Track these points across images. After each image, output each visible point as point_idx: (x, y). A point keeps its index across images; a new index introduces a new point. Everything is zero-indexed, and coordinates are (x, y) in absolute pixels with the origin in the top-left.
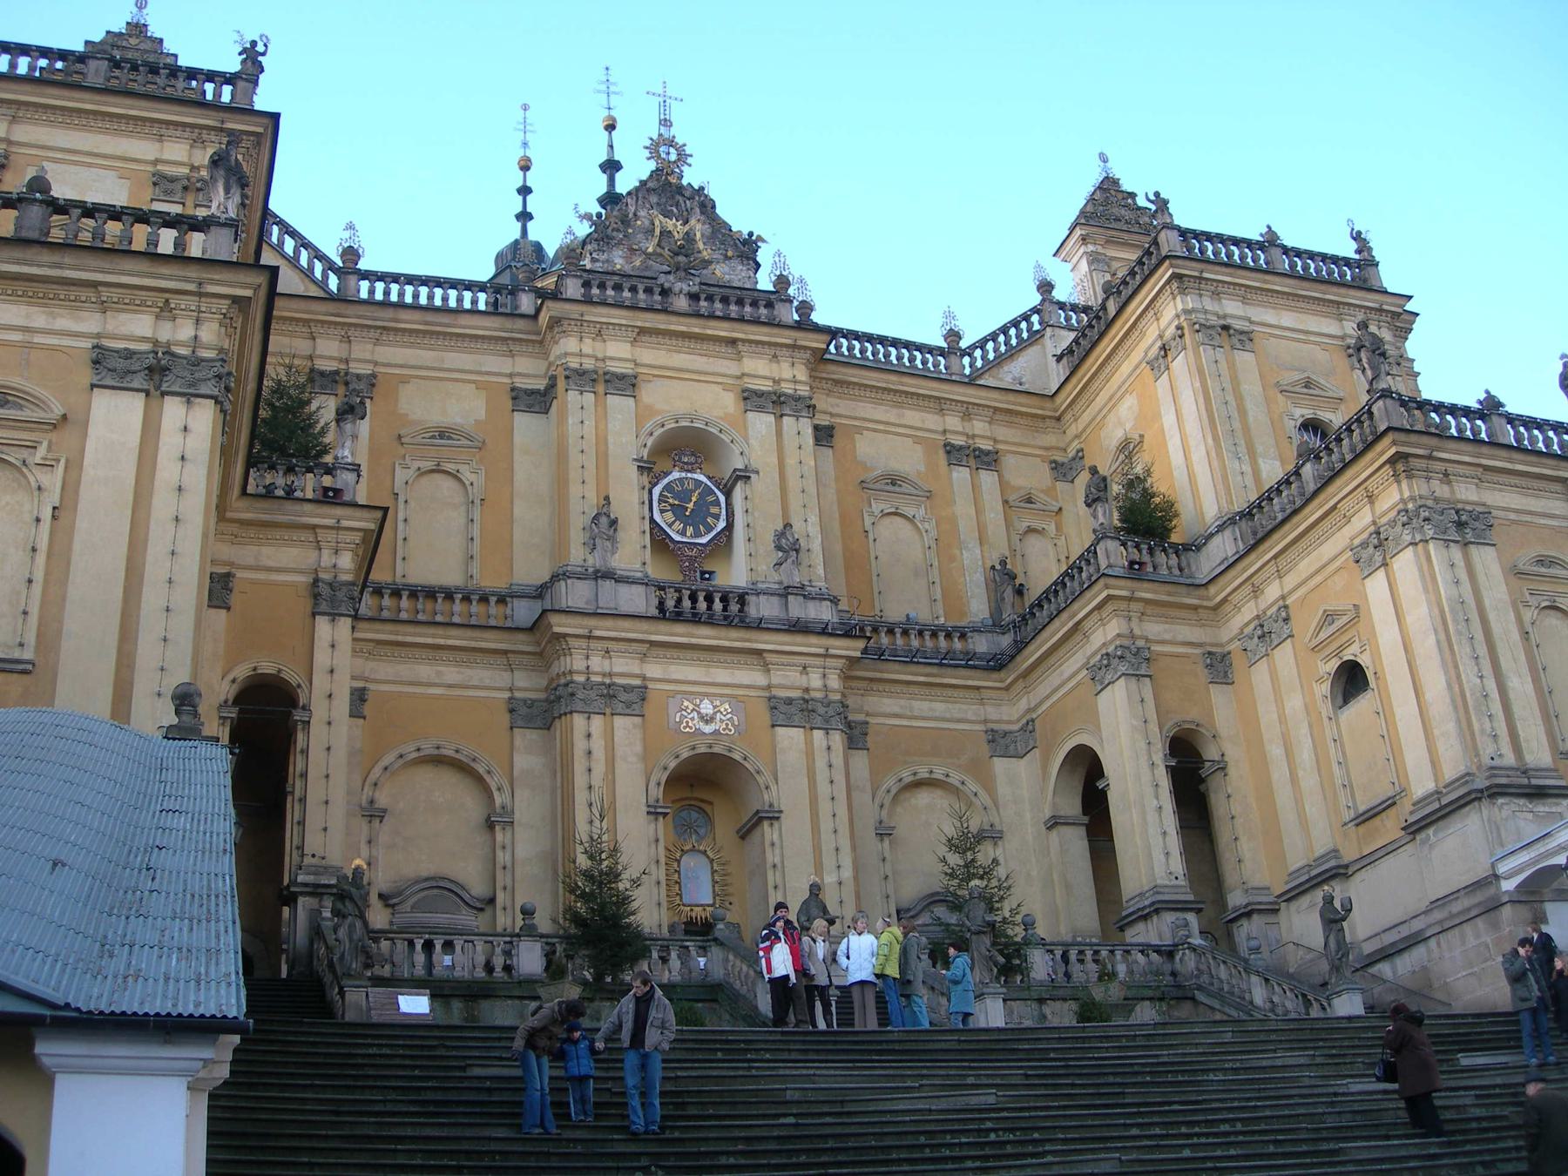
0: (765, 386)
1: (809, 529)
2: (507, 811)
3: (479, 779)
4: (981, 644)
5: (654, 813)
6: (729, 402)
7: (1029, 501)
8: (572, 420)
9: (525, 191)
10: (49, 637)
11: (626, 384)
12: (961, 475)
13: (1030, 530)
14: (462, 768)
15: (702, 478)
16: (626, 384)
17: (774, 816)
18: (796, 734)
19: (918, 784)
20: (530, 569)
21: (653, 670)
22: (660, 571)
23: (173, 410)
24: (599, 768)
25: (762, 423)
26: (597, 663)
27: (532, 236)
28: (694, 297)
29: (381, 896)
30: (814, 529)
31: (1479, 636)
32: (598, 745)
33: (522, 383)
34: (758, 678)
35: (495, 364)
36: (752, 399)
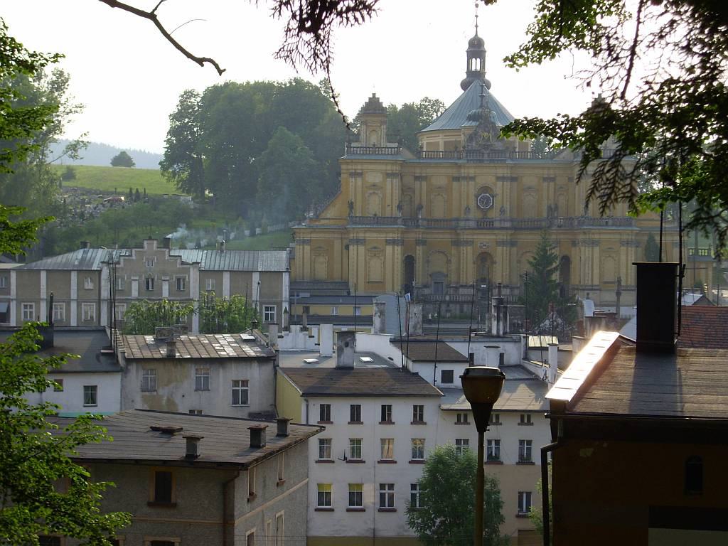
0: (501, 175)
1: (507, 206)
2: (450, 260)
3: (446, 255)
4: (544, 224)
5: (474, 263)
6: (493, 179)
7: (561, 188)
8: (463, 187)
9: (477, 16)
10: (384, 279)
11: (473, 178)
12: (546, 184)
13: (560, 194)
14: (443, 253)
15: (488, 195)
16: (473, 178)
17: (495, 263)
18: (500, 248)
19: (526, 252)
20: (455, 215)
21: (475, 237)
22: (479, 215)
23: (396, 247)
24: (465, 255)
25: (499, 184)
26: (465, 237)
27: (480, 35)
28: (488, 154)
29: (430, 275)
30: (508, 207)
31: (590, 263)
32: (465, 252)
33: (455, 175)
34: (494, 237)
35: (450, 171)
36: (498, 179)
